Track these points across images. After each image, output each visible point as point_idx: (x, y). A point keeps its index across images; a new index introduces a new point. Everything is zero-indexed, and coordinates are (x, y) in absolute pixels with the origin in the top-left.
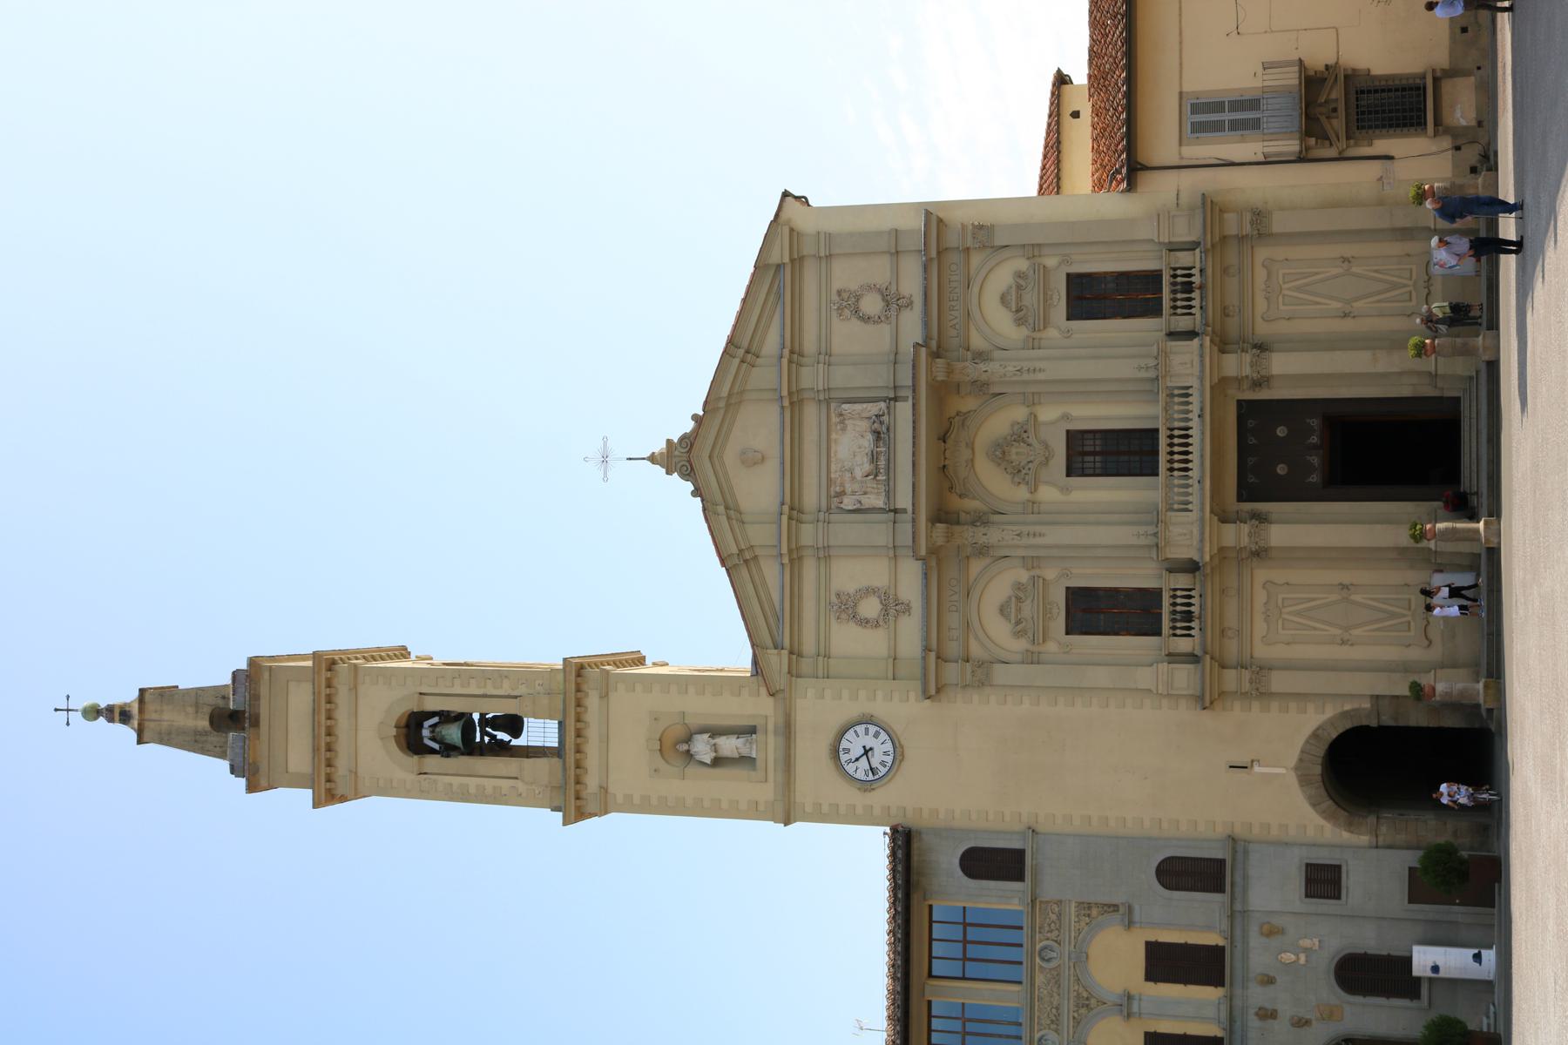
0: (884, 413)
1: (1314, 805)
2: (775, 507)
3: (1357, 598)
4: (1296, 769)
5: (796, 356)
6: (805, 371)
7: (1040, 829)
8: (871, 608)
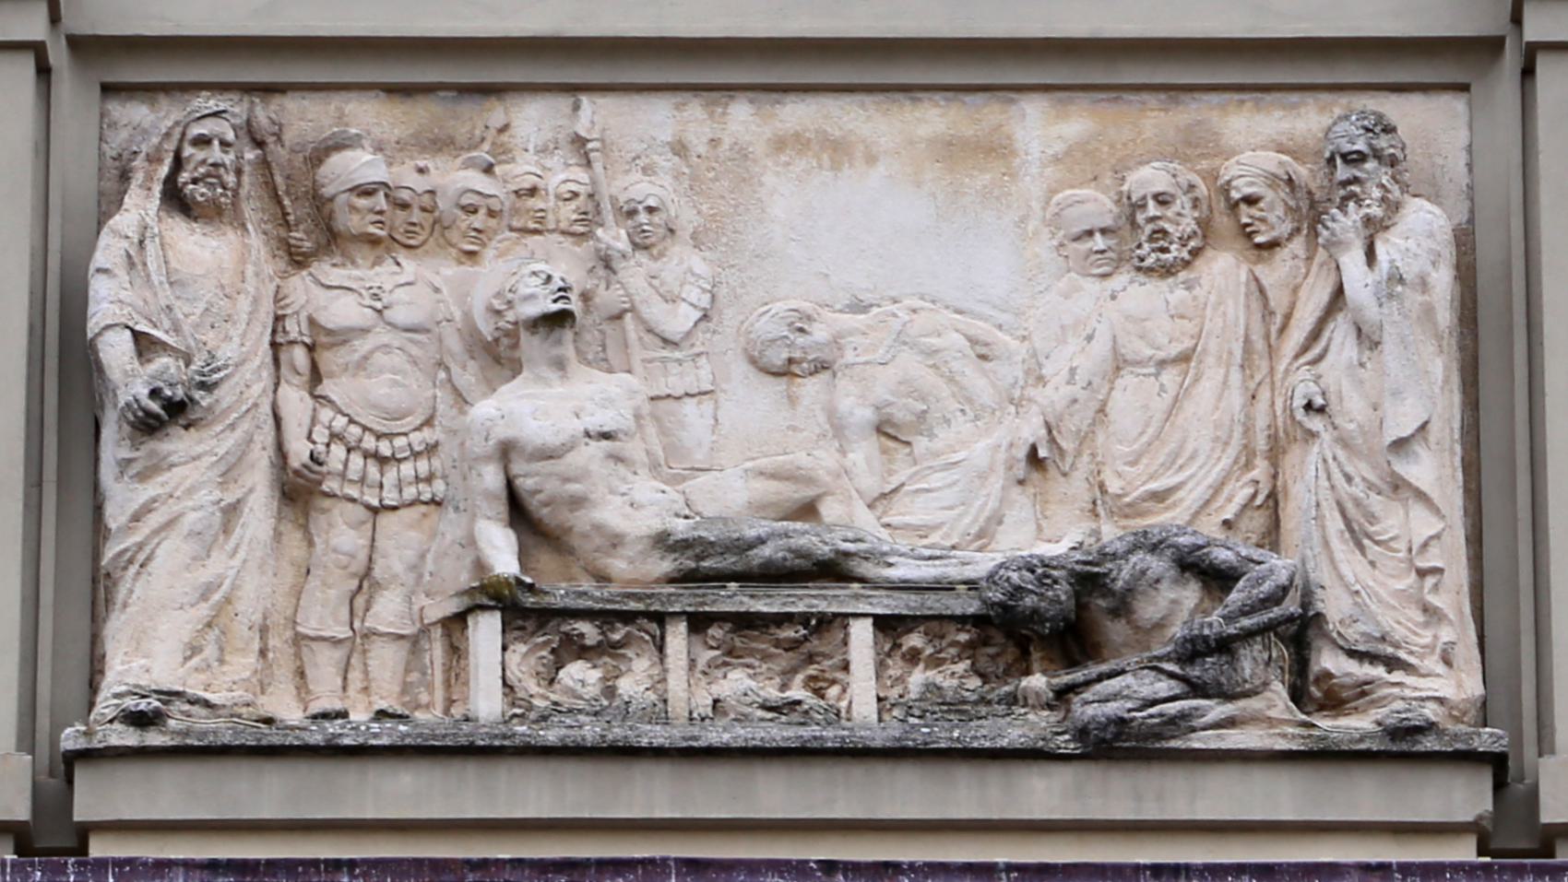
0: (1335, 701)
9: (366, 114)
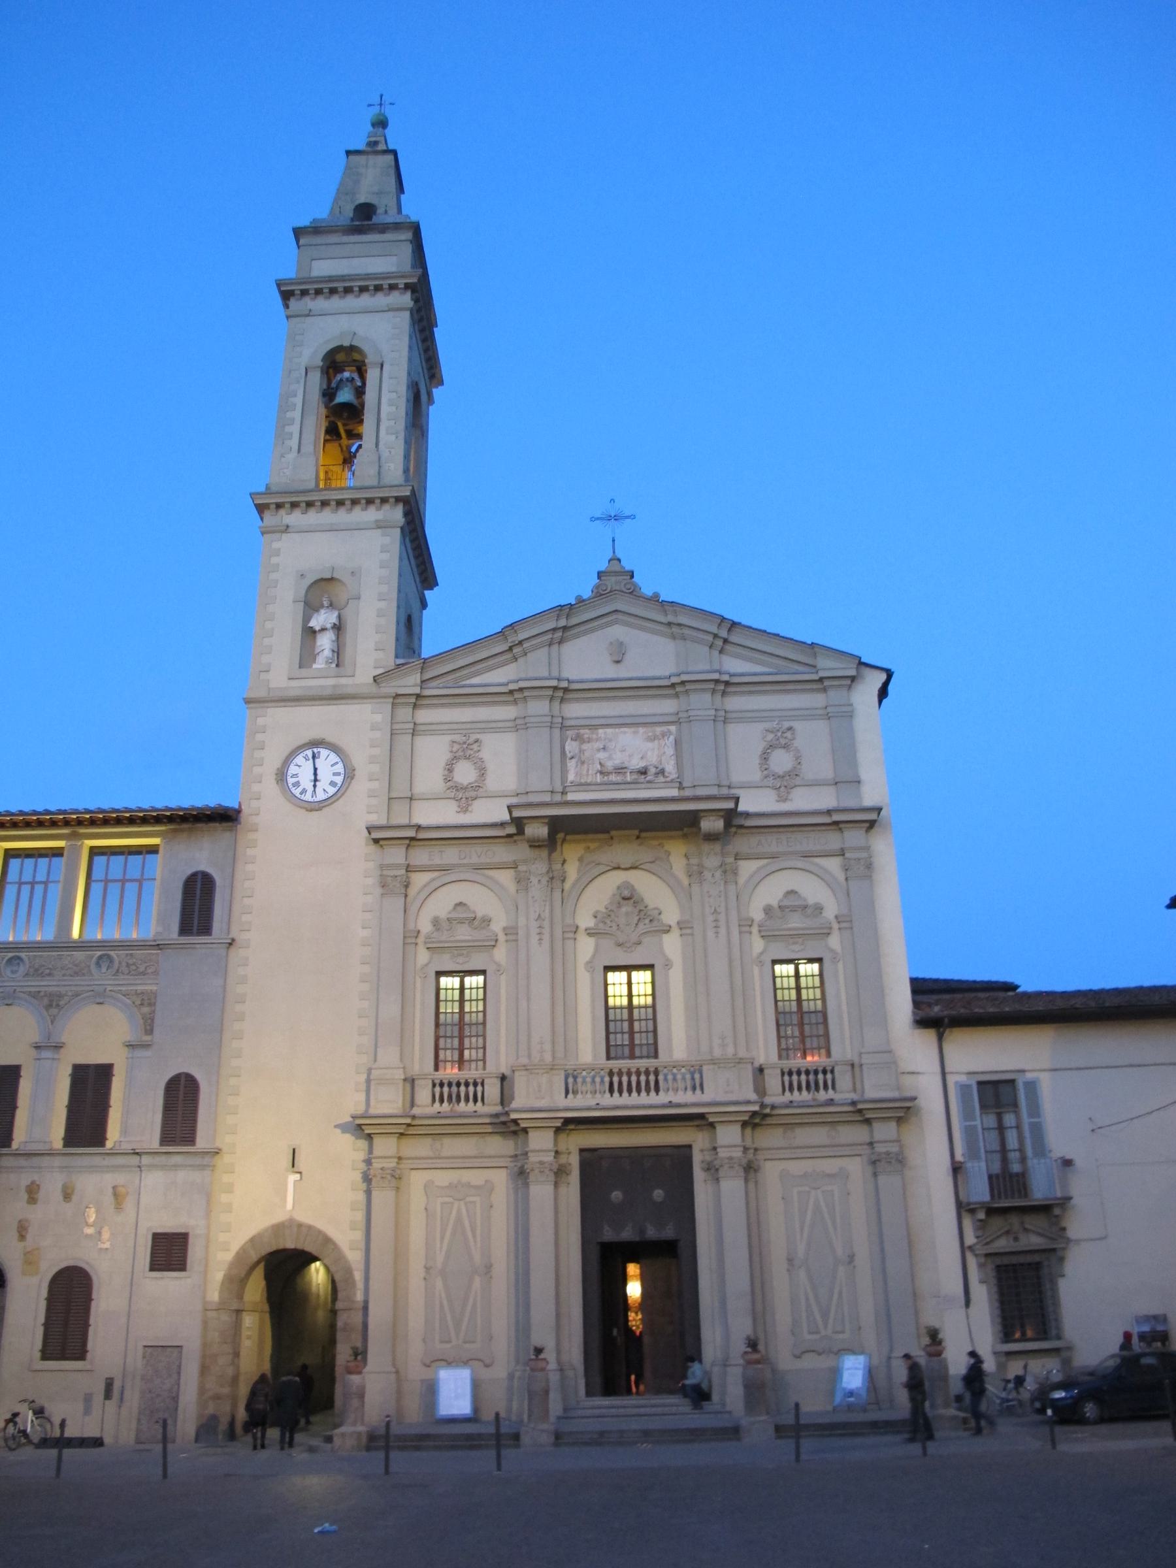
0: (667, 777)
1: (252, 1240)
2: (565, 675)
3: (477, 1282)
4: (291, 1221)
5: (722, 688)
6: (707, 697)
7: (233, 950)
8: (465, 773)
9: (587, 731)
